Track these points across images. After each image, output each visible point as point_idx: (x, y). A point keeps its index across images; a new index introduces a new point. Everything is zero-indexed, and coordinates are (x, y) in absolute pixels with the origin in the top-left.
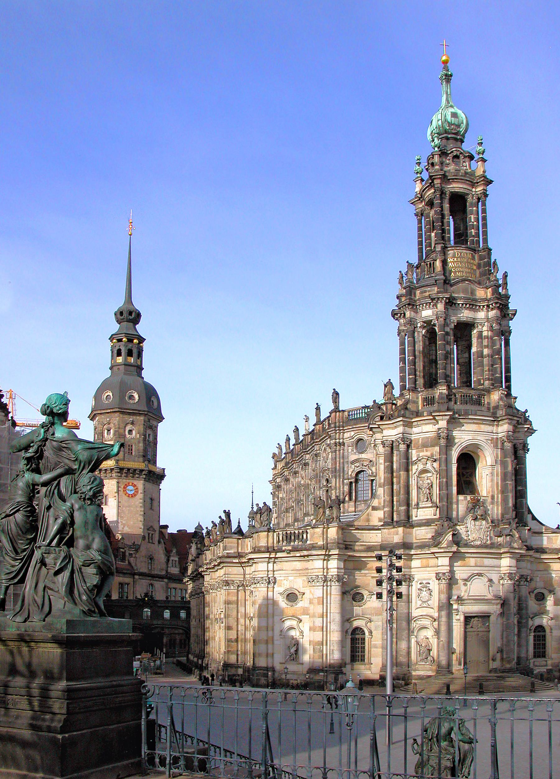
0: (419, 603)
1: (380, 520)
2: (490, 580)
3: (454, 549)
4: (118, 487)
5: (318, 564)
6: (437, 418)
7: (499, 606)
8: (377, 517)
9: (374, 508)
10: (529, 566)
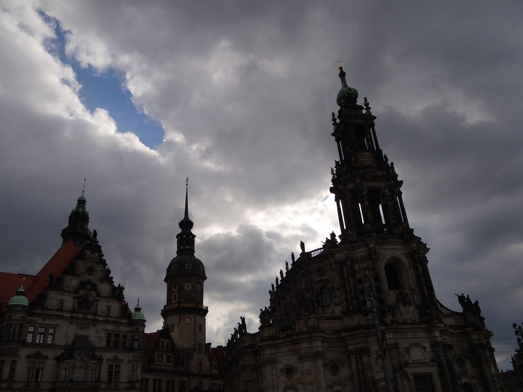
0: (378, 368)
1: (341, 312)
2: (425, 348)
3: (396, 326)
4: (180, 319)
5: (305, 345)
6: (367, 242)
7: (436, 368)
8: (338, 310)
9: (336, 305)
10: (447, 338)
